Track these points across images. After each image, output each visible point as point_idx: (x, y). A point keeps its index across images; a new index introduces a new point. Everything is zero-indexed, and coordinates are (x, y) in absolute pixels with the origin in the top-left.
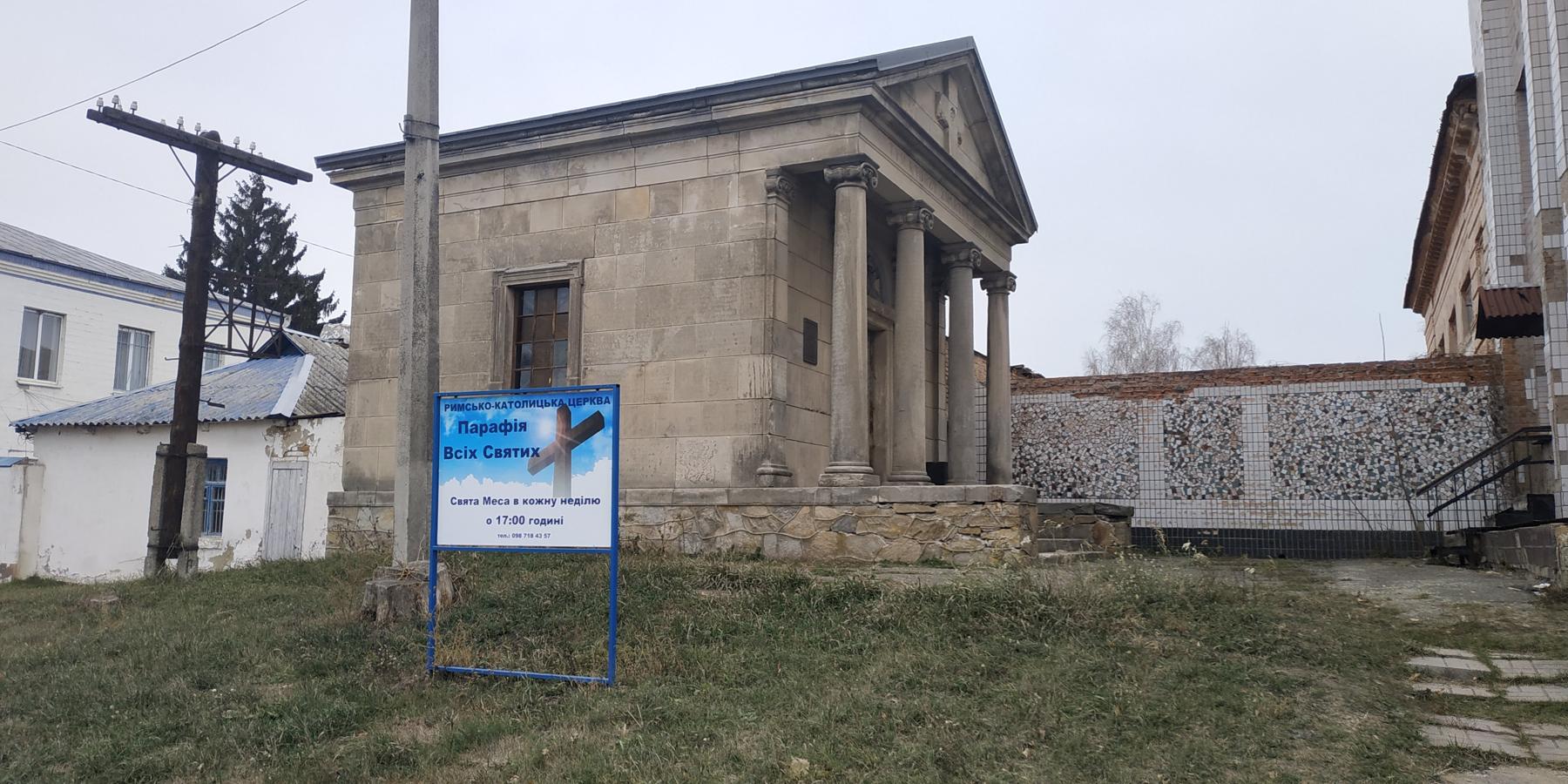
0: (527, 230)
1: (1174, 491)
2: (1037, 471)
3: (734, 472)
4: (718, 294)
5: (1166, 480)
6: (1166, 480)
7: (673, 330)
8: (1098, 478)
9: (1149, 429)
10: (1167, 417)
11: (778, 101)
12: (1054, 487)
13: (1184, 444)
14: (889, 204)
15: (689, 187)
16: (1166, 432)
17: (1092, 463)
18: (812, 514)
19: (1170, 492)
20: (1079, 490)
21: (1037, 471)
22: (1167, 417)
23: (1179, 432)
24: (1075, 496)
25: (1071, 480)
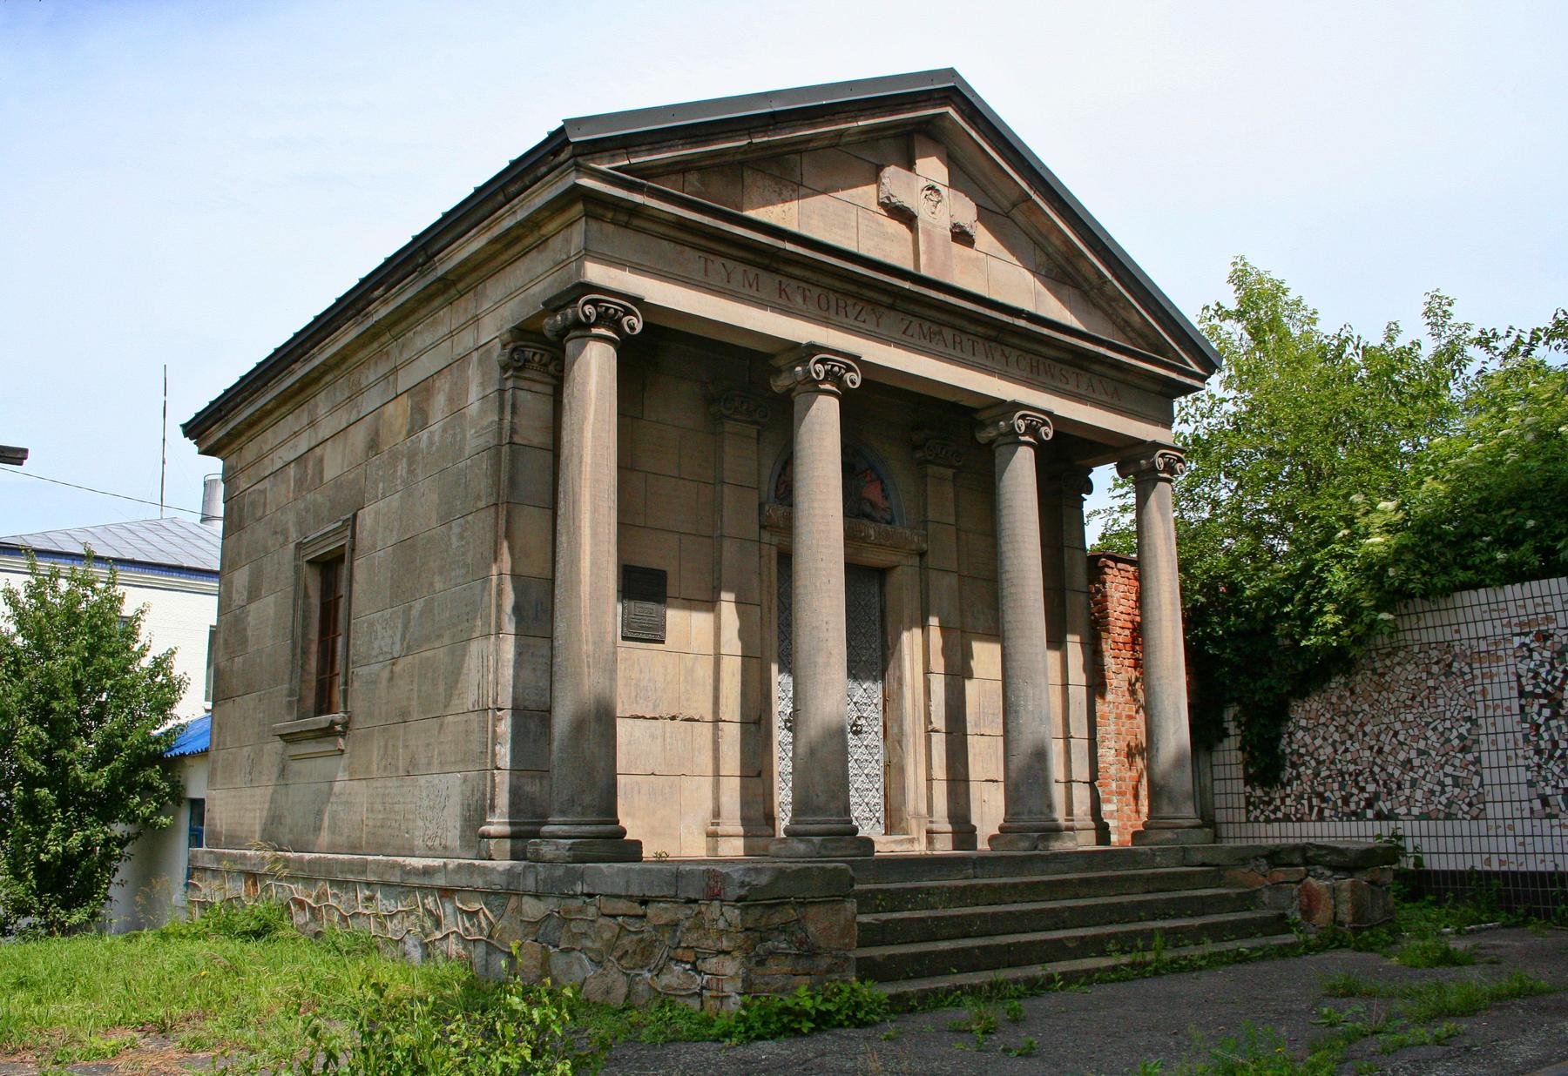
0: (321, 479)
1: (1545, 801)
2: (1317, 775)
3: (462, 837)
4: (455, 542)
5: (1530, 784)
6: (1530, 784)
7: (418, 606)
8: (1414, 783)
9: (1494, 692)
10: (1523, 668)
11: (489, 227)
12: (1346, 801)
13: (1555, 715)
14: (773, 356)
15: (438, 384)
16: (1522, 694)
17: (1402, 756)
18: (518, 910)
19: (1537, 804)
20: (1384, 806)
21: (1317, 775)
22: (1523, 668)
23: (1546, 694)
24: (1379, 816)
25: (1371, 788)
